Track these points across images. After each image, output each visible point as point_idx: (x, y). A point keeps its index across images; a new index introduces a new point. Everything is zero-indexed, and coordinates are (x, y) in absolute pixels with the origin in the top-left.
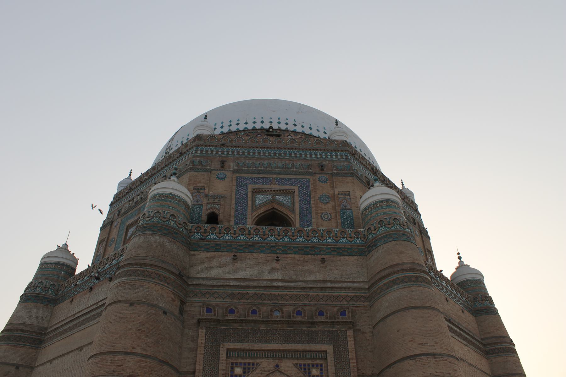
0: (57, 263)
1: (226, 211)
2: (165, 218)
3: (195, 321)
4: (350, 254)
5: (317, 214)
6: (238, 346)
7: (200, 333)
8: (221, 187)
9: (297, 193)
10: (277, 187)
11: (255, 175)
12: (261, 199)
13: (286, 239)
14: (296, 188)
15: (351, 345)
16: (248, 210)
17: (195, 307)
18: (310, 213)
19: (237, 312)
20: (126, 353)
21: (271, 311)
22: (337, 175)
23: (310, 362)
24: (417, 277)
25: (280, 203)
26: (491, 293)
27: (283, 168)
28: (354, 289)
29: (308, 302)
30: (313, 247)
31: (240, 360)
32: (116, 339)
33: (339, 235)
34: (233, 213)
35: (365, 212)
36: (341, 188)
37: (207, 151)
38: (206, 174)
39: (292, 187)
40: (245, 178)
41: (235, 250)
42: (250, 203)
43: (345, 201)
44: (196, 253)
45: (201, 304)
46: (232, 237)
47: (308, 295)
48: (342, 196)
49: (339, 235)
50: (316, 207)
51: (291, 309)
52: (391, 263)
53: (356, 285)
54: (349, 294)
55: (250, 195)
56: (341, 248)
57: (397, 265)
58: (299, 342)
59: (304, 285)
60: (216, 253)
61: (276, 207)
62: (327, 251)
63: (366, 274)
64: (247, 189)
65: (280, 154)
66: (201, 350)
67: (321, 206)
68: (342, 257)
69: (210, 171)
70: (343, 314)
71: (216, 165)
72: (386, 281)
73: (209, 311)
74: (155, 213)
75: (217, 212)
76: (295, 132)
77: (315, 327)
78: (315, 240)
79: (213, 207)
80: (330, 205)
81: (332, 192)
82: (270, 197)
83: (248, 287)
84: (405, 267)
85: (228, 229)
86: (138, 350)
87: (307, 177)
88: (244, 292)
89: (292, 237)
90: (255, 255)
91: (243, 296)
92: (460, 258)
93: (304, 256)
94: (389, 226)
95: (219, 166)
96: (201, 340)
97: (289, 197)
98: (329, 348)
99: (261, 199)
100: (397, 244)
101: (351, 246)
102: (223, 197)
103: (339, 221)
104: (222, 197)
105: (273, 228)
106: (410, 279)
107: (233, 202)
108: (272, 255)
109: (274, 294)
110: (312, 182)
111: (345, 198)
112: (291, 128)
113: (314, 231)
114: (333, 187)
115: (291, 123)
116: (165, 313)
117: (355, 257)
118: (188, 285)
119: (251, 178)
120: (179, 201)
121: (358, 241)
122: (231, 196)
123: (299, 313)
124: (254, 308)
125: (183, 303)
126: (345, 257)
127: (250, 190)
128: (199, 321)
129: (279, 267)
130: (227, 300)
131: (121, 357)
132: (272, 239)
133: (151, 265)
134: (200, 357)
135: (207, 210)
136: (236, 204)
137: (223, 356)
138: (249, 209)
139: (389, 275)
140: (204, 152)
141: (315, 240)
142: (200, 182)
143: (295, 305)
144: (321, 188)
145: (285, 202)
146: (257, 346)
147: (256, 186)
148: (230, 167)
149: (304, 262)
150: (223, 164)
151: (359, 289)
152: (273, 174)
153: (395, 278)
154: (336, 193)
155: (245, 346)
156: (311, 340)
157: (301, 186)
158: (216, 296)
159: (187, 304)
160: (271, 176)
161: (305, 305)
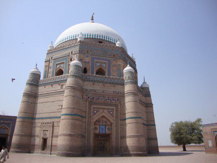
1: (89, 67)
4: (121, 85)
6: (95, 106)
8: (87, 59)
9: (107, 63)
10: (102, 61)
11: (97, 57)
12: (98, 64)
14: (107, 62)
18: (110, 70)
25: (102, 66)
34: (91, 68)
41: (94, 82)
42: (95, 65)
50: (112, 68)
55: (95, 63)
66: (87, 107)
75: (86, 67)
76: (106, 40)
86: (76, 108)
87: (110, 59)
90: (98, 83)
92: (144, 80)
96: (87, 105)
98: (115, 108)
107: (91, 65)
110: (111, 60)
115: (106, 37)
131: (73, 109)
134: (87, 108)
137: (92, 108)
150: (88, 52)
156: (111, 106)
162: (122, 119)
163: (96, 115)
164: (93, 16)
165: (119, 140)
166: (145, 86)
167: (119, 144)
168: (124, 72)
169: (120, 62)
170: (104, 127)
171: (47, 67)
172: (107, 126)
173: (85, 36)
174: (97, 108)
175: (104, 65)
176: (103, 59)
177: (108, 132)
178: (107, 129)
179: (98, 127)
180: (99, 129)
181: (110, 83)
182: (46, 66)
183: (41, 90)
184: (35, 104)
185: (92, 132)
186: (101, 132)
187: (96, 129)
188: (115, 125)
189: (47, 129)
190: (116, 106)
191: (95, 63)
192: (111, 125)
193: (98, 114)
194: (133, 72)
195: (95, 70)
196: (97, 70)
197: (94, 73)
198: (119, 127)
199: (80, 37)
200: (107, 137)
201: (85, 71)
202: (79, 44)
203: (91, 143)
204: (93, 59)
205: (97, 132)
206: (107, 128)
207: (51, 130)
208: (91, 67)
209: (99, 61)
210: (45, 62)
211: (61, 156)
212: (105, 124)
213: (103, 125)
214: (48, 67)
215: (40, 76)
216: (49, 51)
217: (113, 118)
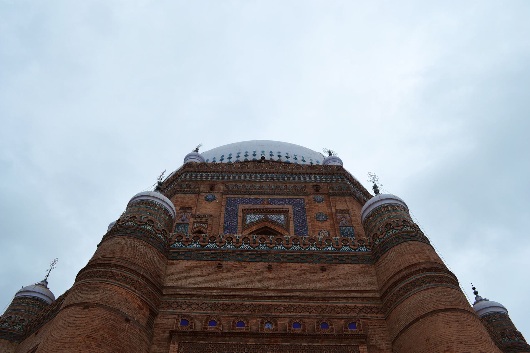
2: (141, 222)
3: (167, 335)
7: (171, 348)
9: (291, 211)
10: (270, 206)
11: (246, 196)
13: (280, 247)
14: (290, 208)
16: (238, 229)
17: (168, 320)
19: (220, 324)
21: (262, 323)
22: (334, 195)
24: (440, 277)
25: (273, 222)
26: (519, 328)
27: (276, 189)
28: (364, 299)
29: (308, 314)
30: (311, 255)
32: (59, 347)
33: (340, 243)
35: (368, 220)
37: (196, 177)
38: (193, 196)
39: (286, 207)
40: (235, 199)
42: (240, 221)
43: (344, 219)
44: (175, 262)
45: (176, 316)
46: (217, 245)
47: (308, 306)
48: (341, 214)
49: (340, 243)
52: (406, 265)
53: (366, 295)
54: (357, 305)
55: (240, 214)
56: (343, 256)
57: (413, 265)
59: (302, 295)
60: (197, 262)
61: (268, 225)
62: (327, 259)
63: (376, 283)
64: (237, 209)
67: (318, 224)
68: (346, 266)
69: (199, 193)
72: (402, 285)
73: (184, 322)
74: (130, 218)
77: (318, 342)
78: (313, 248)
79: (200, 226)
80: (327, 224)
81: (330, 211)
82: (262, 216)
83: (234, 297)
84: (424, 266)
85: (213, 239)
87: (301, 197)
88: (230, 302)
89: (286, 246)
90: (243, 264)
91: (227, 307)
92: (476, 293)
93: (300, 264)
94: (399, 228)
95: (209, 189)
97: (283, 216)
99: (251, 218)
100: (410, 245)
101: (355, 254)
102: (211, 217)
104: (210, 216)
106: (432, 279)
107: (222, 220)
108: (264, 263)
109: (267, 305)
110: (307, 201)
111: (344, 216)
114: (330, 207)
116: (127, 320)
117: (361, 265)
118: (163, 295)
119: (242, 199)
120: (159, 209)
121: (363, 249)
122: (220, 215)
123: (297, 325)
124: (241, 319)
125: (154, 314)
126: (349, 265)
127: (240, 209)
128: (172, 334)
129: (270, 276)
130: (209, 312)
132: (263, 247)
133: (117, 266)
135: (193, 228)
136: (225, 223)
138: (239, 227)
139: (403, 278)
140: (193, 177)
141: (313, 248)
142: (187, 203)
143: (291, 317)
144: (317, 208)
145: (278, 221)
147: (246, 206)
148: (220, 189)
149: (301, 271)
150: (212, 188)
151: (370, 299)
153: (413, 279)
154: (334, 211)
157: (295, 205)
158: (194, 307)
159: (159, 316)
160: (263, 197)
161: (304, 317)
175: (280, 219)
176: (273, 202)
208: (225, 229)
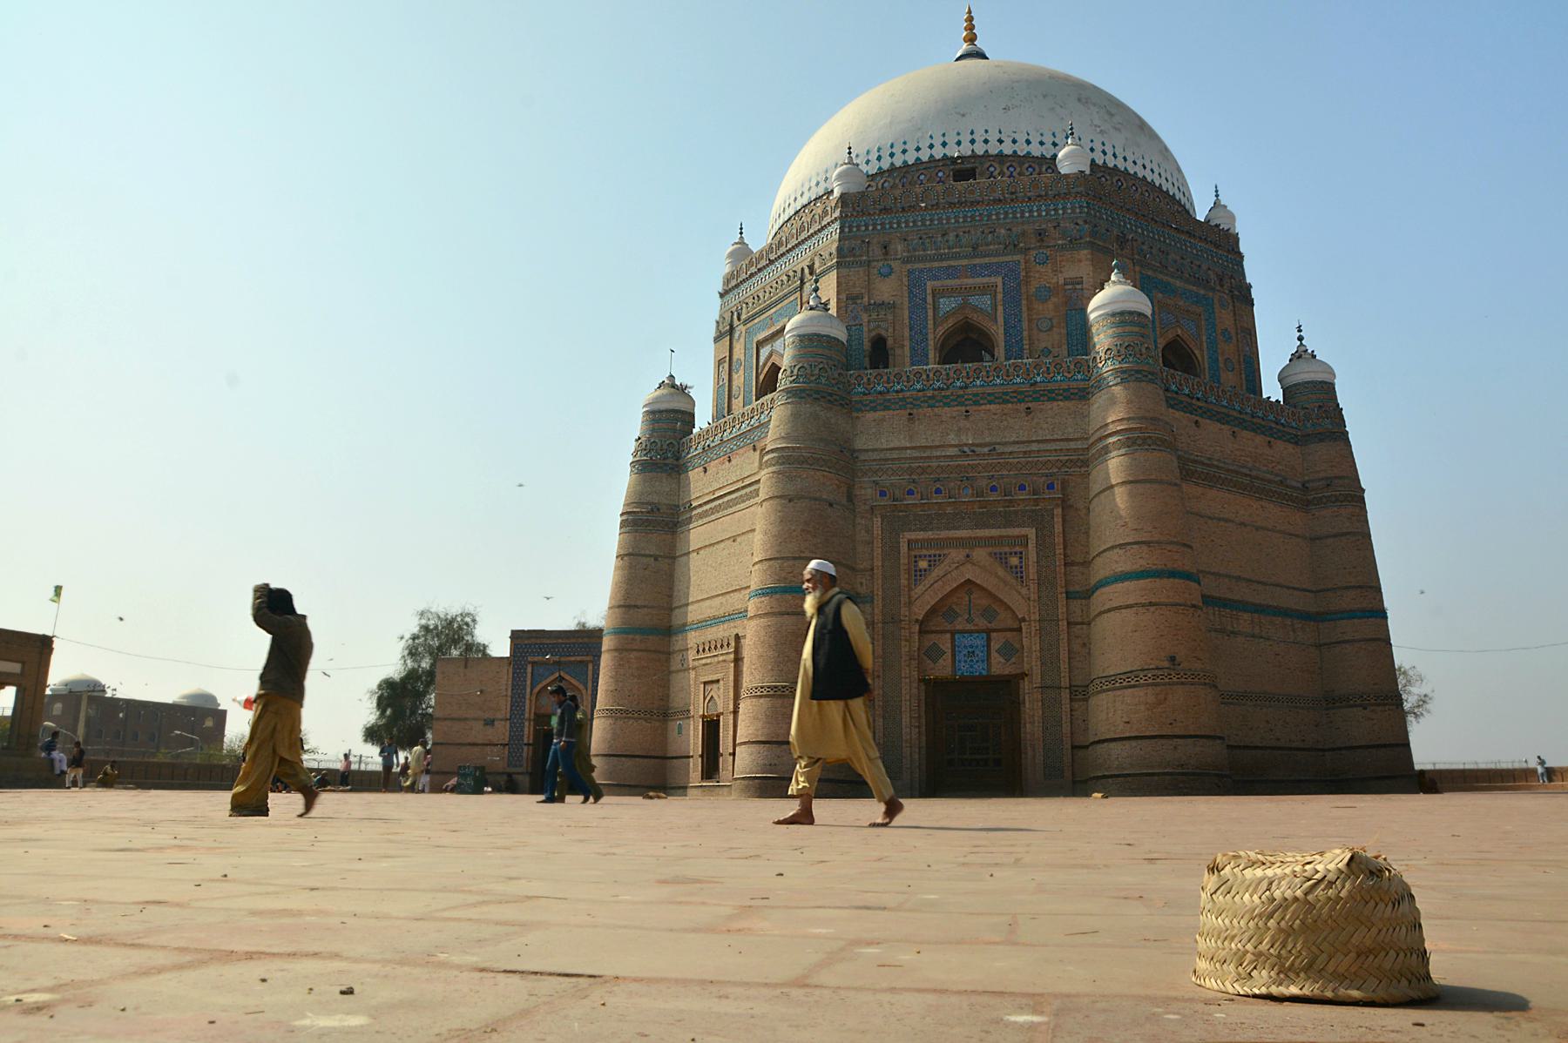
0: (667, 411)
4: (1067, 398)
5: (1030, 321)
6: (921, 535)
8: (886, 290)
9: (1000, 289)
11: (936, 264)
12: (947, 304)
14: (999, 280)
15: (1058, 528)
17: (866, 491)
20: (794, 558)
23: (1007, 549)
24: (1144, 439)
25: (975, 309)
31: (924, 552)
34: (907, 334)
36: (1070, 272)
37: (858, 227)
40: (921, 271)
51: (984, 483)
55: (929, 299)
58: (993, 526)
65: (973, 217)
70: (1051, 487)
71: (877, 251)
73: (883, 494)
75: (883, 333)
76: (1000, 155)
91: (924, 471)
92: (1300, 339)
96: (877, 531)
98: (1031, 533)
103: (1064, 331)
105: (959, 365)
107: (906, 313)
112: (994, 149)
113: (1016, 366)
119: (930, 270)
125: (850, 488)
127: (929, 291)
134: (878, 552)
137: (904, 548)
146: (944, 534)
152: (960, 258)
155: (930, 535)
162: (1077, 588)
163: (927, 582)
164: (970, 19)
165: (1066, 707)
166: (1305, 374)
167: (1066, 728)
168: (1092, 317)
169: (1080, 266)
170: (979, 641)
171: (726, 364)
172: (994, 635)
173: (879, 159)
174: (929, 543)
175: (985, 302)
176: (974, 271)
177: (999, 666)
178: (994, 654)
179: (945, 642)
180: (949, 654)
181: (1002, 399)
182: (720, 363)
183: (701, 484)
184: (674, 558)
185: (905, 672)
186: (964, 669)
187: (934, 653)
188: (1035, 626)
189: (715, 678)
190: (1039, 520)
191: (929, 299)
192: (1020, 630)
193: (937, 572)
194: (1140, 314)
195: (933, 337)
196: (948, 336)
197: (927, 356)
198: (1064, 636)
199: (839, 177)
200: (1003, 690)
201: (880, 353)
202: (837, 214)
203: (905, 730)
204: (914, 285)
205: (942, 668)
206: (995, 646)
207: (732, 678)
209: (949, 282)
210: (717, 340)
211: (761, 796)
212: (982, 623)
213: (971, 632)
214: (726, 365)
215: (688, 418)
216: (727, 281)
217: (1024, 591)
